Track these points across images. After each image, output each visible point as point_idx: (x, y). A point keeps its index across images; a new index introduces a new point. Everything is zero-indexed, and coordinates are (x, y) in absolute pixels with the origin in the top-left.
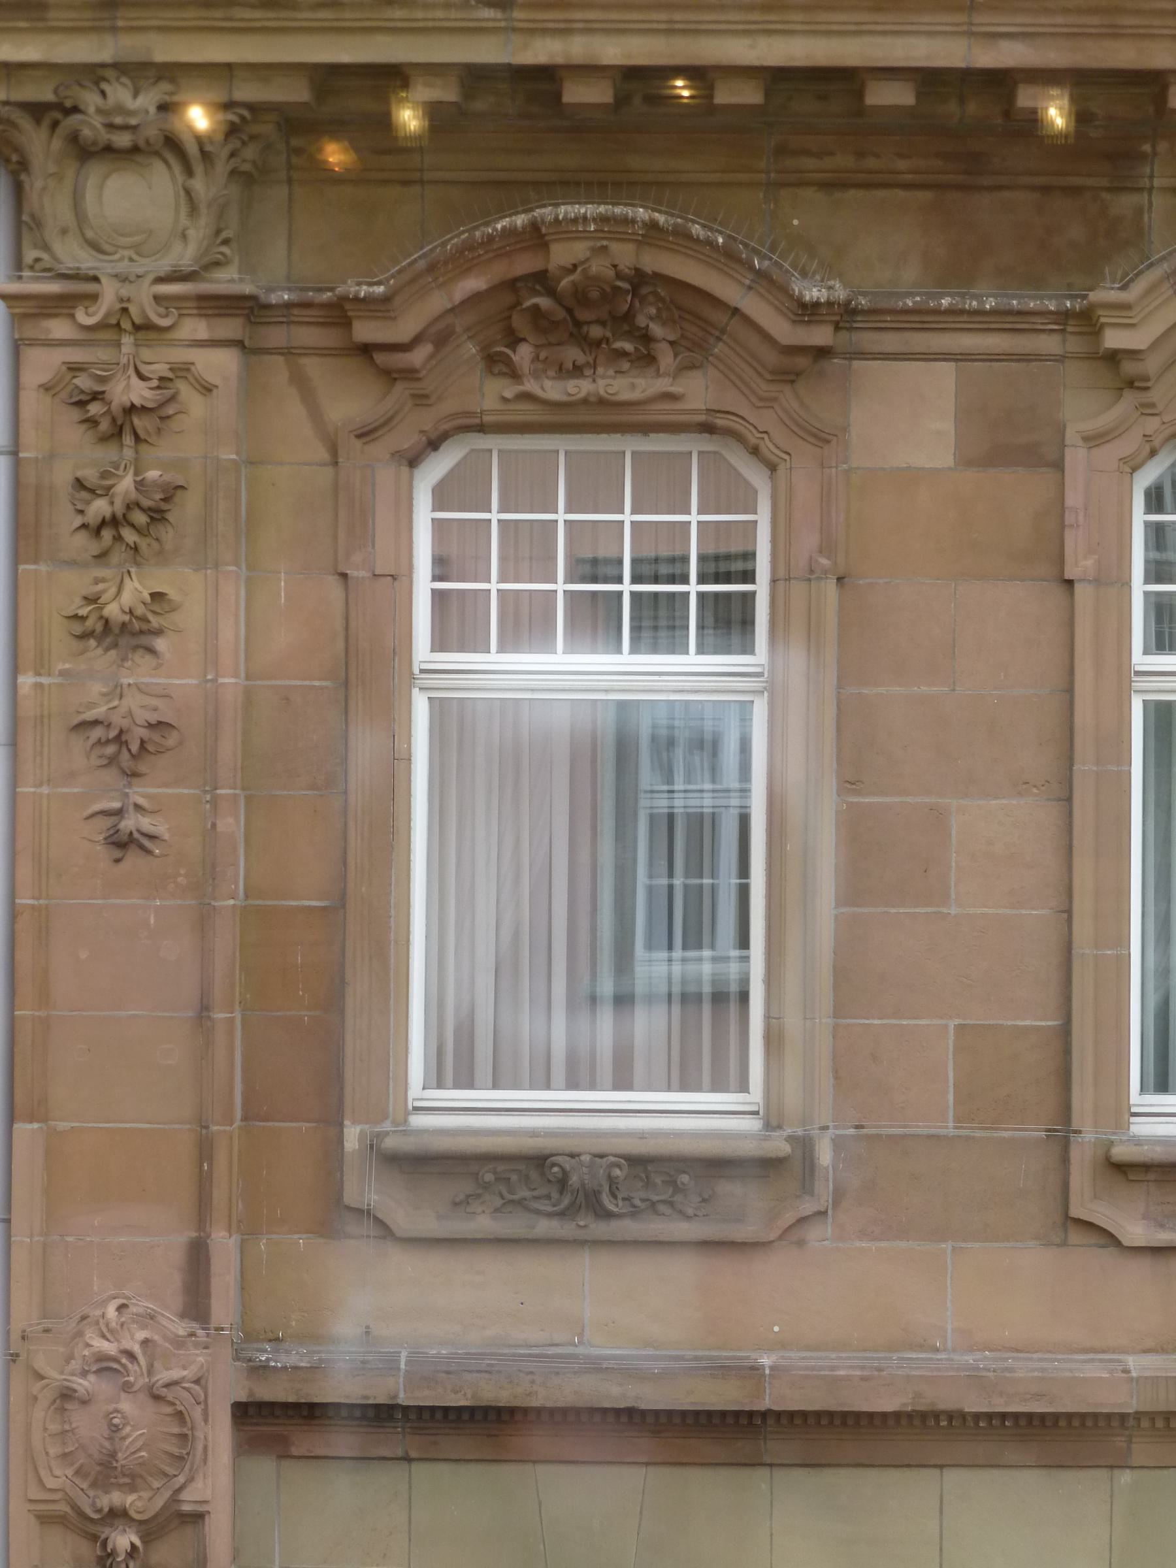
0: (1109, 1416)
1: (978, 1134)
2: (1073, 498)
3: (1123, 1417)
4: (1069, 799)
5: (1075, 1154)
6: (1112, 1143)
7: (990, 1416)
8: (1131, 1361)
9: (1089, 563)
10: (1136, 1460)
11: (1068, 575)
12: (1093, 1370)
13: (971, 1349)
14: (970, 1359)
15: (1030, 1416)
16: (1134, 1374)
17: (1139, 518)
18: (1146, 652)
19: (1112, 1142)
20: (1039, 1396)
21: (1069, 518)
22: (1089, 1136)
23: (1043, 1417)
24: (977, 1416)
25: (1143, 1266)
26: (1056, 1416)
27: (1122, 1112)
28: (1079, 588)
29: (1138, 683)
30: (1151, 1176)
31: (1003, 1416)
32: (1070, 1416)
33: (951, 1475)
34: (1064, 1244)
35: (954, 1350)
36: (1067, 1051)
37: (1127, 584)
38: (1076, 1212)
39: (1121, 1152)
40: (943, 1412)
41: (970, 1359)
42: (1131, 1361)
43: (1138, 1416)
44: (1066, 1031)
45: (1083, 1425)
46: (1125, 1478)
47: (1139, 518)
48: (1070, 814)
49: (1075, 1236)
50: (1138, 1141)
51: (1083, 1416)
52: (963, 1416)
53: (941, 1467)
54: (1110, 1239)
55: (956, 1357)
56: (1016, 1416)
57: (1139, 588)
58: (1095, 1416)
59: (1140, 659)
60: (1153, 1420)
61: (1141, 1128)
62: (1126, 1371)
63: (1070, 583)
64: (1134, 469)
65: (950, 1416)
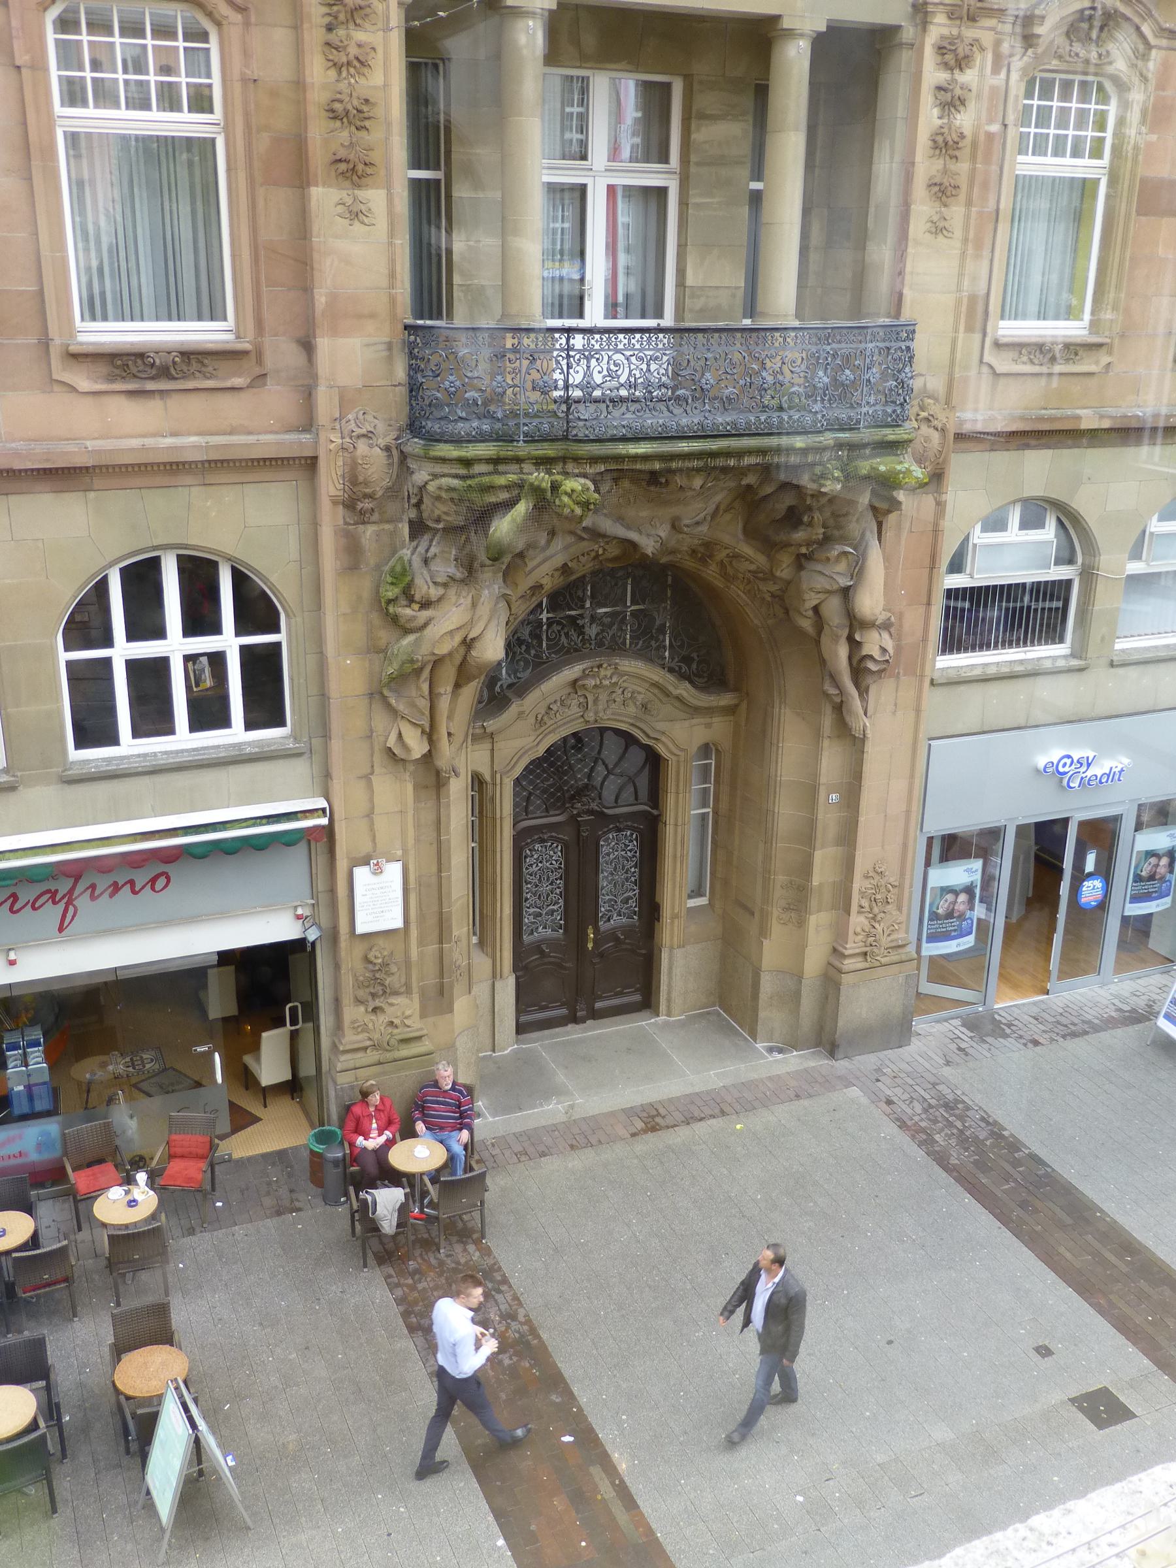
0: (81, 468)
1: (5, 342)
2: (15, 23)
3: (87, 468)
4: (30, 179)
5: (52, 349)
6: (69, 345)
7: (26, 471)
8: (89, 443)
9: (27, 57)
10: (96, 487)
11: (18, 63)
12: (71, 447)
13: (14, 441)
14: (13, 445)
15: (45, 469)
16: (90, 449)
17: (51, 37)
18: (62, 105)
19: (69, 345)
20: (47, 460)
21: (14, 33)
22: (57, 341)
23: (50, 469)
24: (20, 471)
25: (89, 400)
26: (57, 469)
27: (71, 331)
28: (24, 71)
29: (59, 122)
30: (88, 360)
31: (32, 470)
32: (63, 469)
33: (11, 498)
34: (52, 392)
35: (6, 442)
36: (43, 301)
37: (46, 69)
38: (55, 377)
39: (73, 349)
40: (5, 470)
41: (13, 445)
42: (89, 443)
43: (94, 467)
44: (41, 293)
45: (70, 473)
46: (92, 495)
47: (51, 37)
48: (32, 186)
49: (56, 388)
50: (81, 344)
51: (69, 468)
52: (14, 471)
53: (7, 494)
54: (73, 389)
55: (8, 445)
56: (38, 470)
57: (54, 73)
58: (75, 468)
59: (58, 109)
60: (107, 469)
61: (82, 338)
62: (86, 448)
63: (19, 67)
64: (45, 9)
65: (8, 471)
